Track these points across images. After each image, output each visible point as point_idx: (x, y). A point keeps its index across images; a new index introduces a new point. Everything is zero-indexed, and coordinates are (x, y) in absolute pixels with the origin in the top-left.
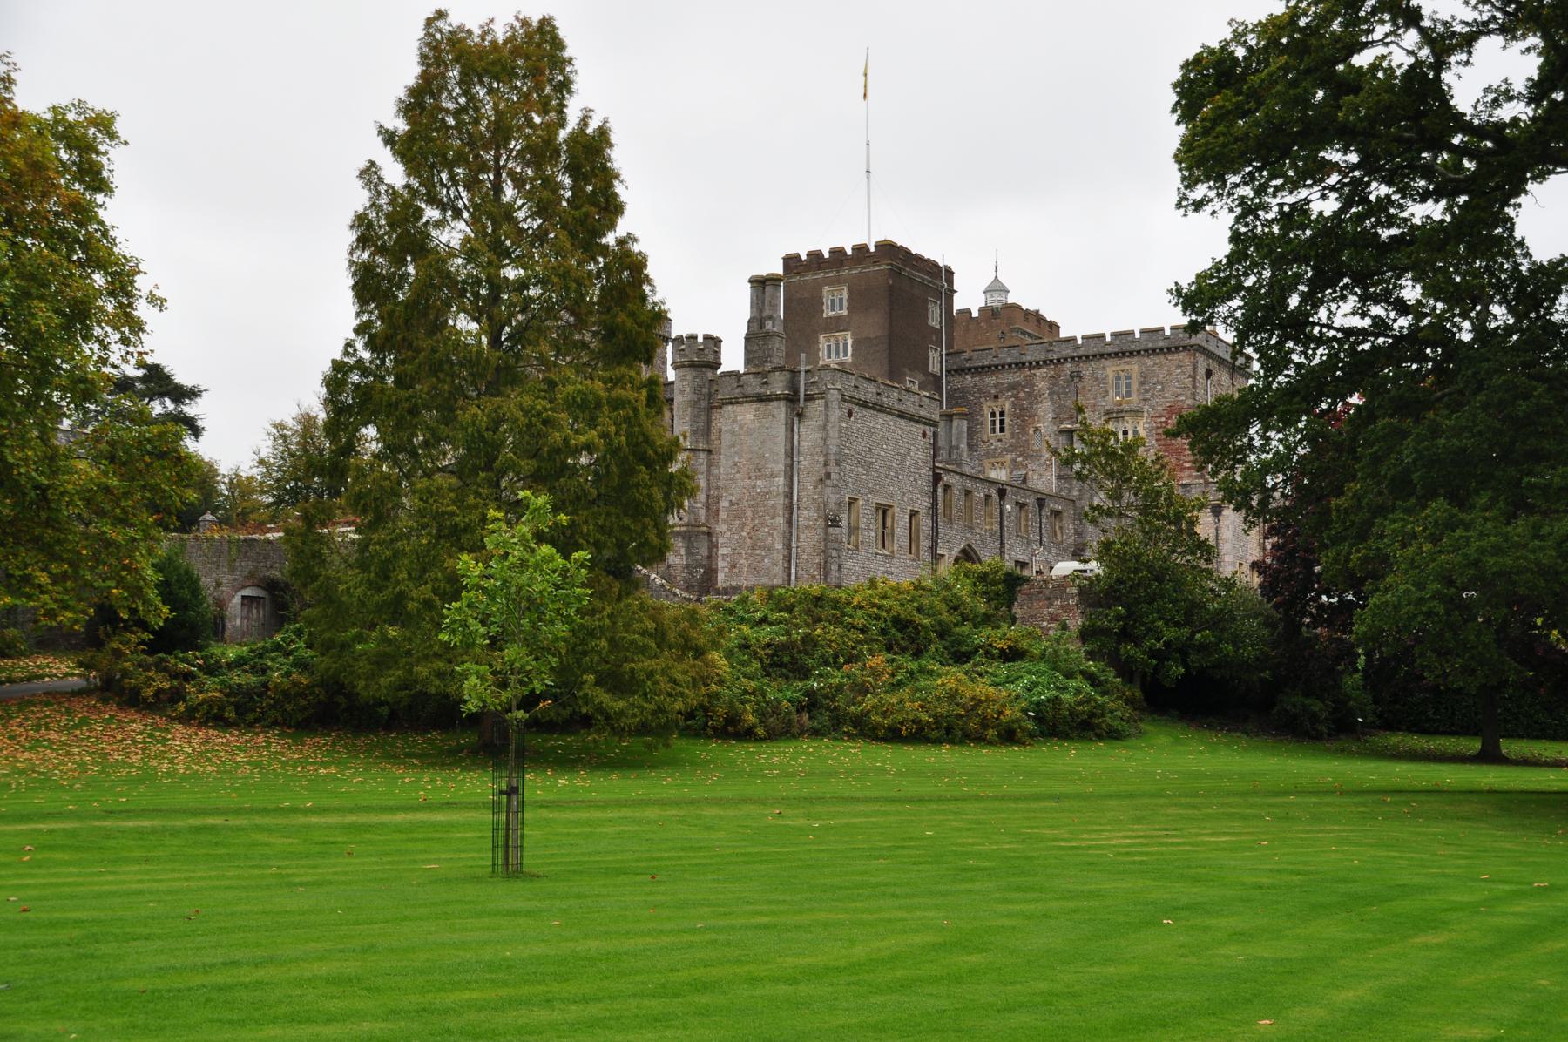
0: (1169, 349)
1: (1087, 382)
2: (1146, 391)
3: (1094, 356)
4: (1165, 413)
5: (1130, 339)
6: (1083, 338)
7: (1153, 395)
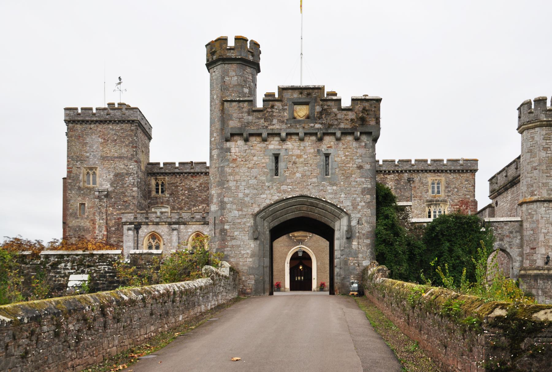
0: (463, 171)
1: (417, 184)
2: (449, 191)
3: (422, 171)
4: (459, 203)
5: (442, 163)
6: (432, 160)
7: (453, 194)
